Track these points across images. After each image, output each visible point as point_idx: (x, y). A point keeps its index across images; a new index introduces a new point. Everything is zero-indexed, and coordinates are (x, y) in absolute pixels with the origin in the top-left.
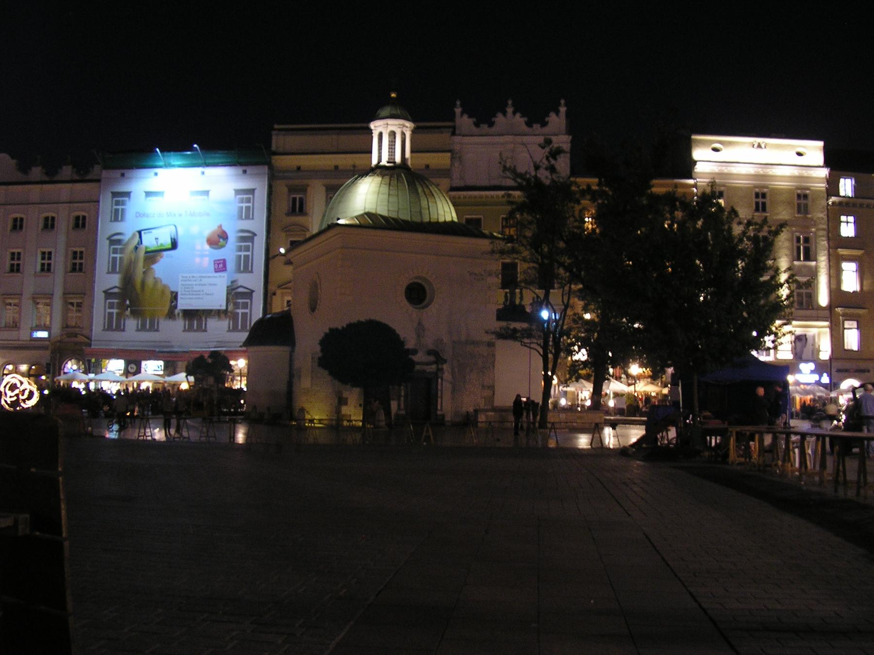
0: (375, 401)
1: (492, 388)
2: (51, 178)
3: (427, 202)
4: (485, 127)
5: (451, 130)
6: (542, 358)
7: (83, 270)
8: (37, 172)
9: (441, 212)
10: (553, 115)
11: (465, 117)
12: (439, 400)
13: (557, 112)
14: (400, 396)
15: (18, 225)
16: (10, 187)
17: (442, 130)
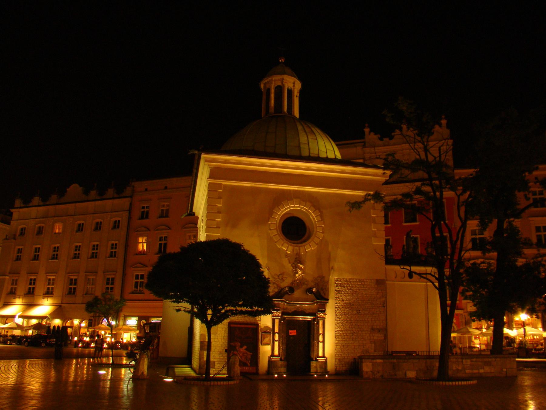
0: (241, 346)
1: (384, 330)
2: (102, 195)
3: (306, 138)
4: (386, 140)
5: (363, 144)
6: (437, 291)
7: (117, 257)
8: (93, 193)
9: (322, 148)
10: (437, 127)
11: (372, 134)
12: (321, 345)
13: (440, 125)
14: (274, 340)
15: (80, 228)
16: (77, 204)
17: (356, 144)
